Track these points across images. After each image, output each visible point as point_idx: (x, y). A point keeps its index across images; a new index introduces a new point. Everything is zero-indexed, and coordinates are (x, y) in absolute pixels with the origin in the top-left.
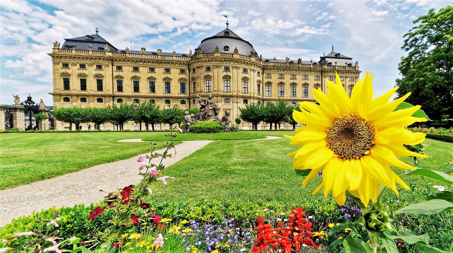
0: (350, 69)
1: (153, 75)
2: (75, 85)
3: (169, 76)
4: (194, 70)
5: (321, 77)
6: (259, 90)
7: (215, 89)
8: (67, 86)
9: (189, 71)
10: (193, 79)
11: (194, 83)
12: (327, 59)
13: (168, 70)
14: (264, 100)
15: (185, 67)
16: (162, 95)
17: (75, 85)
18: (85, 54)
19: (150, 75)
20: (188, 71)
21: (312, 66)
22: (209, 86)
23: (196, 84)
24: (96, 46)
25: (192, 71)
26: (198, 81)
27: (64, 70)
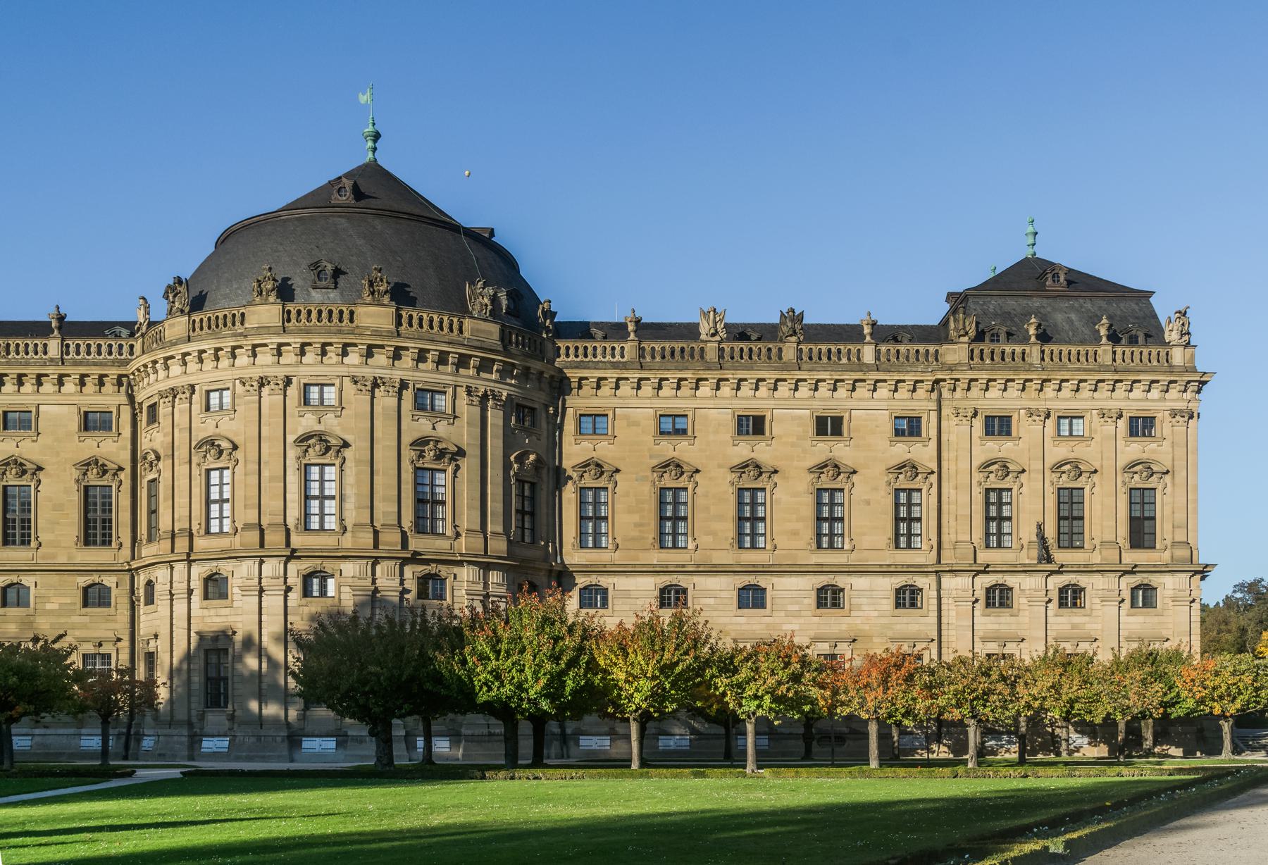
5: (934, 415)
7: (252, 517)
9: (134, 416)
15: (111, 399)
21: (868, 353)
22: (222, 501)
25: (144, 417)
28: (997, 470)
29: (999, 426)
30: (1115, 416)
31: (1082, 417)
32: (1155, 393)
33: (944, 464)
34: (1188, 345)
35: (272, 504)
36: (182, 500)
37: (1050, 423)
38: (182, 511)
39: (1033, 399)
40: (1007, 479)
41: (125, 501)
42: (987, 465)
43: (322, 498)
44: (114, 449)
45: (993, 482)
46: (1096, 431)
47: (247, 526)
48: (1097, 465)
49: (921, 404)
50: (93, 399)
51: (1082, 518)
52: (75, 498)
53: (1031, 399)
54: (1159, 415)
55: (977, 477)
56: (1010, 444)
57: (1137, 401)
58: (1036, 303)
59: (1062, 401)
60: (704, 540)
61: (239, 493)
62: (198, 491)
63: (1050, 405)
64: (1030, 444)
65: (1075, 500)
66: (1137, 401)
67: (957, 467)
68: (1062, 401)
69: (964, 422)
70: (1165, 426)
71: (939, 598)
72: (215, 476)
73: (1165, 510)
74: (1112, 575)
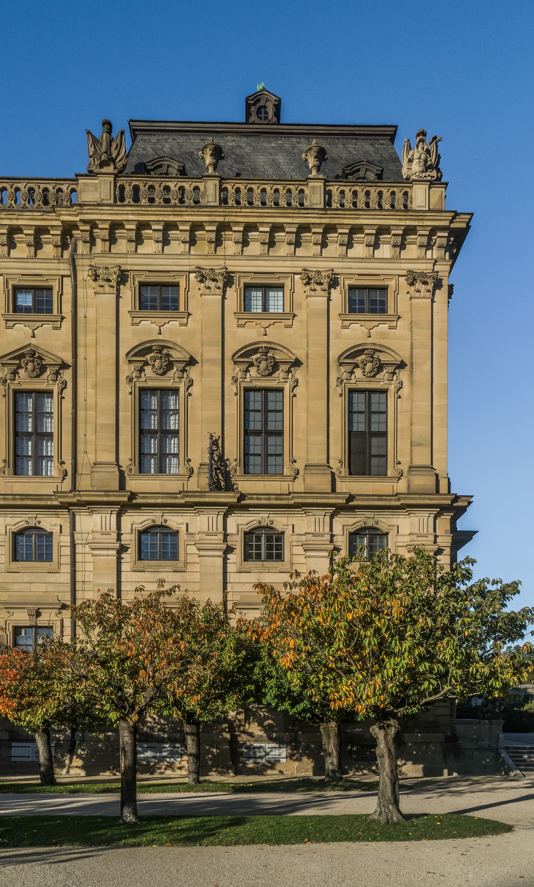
28: (154, 359)
29: (160, 296)
30: (326, 281)
31: (280, 287)
32: (385, 251)
33: (81, 351)
37: (233, 294)
39: (206, 257)
40: (170, 374)
42: (142, 351)
45: (150, 378)
46: (300, 306)
48: (301, 354)
49: (48, 264)
51: (280, 433)
53: (202, 256)
54: (392, 283)
55: (126, 370)
56: (174, 324)
57: (358, 262)
59: (251, 261)
63: (233, 266)
64: (202, 324)
65: (271, 406)
66: (358, 262)
67: (97, 355)
68: (251, 261)
69: (107, 289)
70: (404, 300)
71: (73, 546)
73: (405, 417)
74: (319, 513)
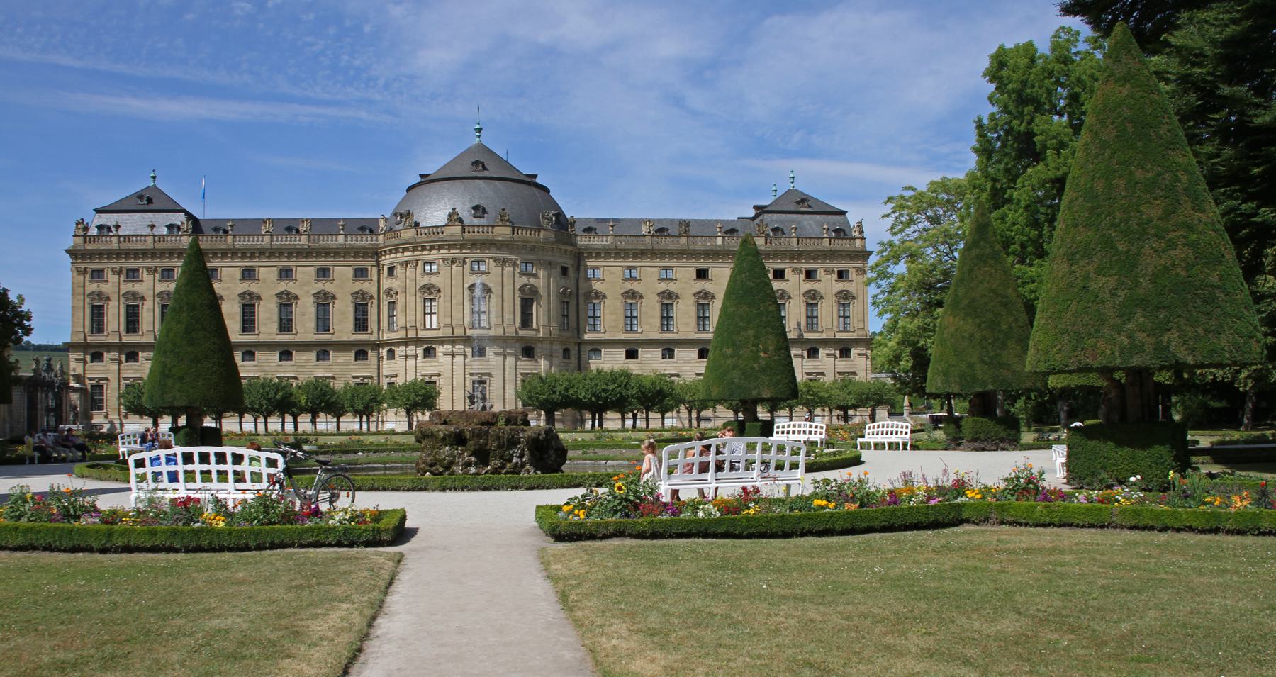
0: (841, 245)
1: (290, 287)
2: (114, 318)
3: (329, 287)
4: (391, 270)
6: (565, 316)
8: (98, 321)
10: (389, 293)
11: (392, 305)
12: (767, 217)
13: (323, 273)
14: (579, 344)
15: (368, 263)
16: (312, 337)
17: (114, 318)
18: (139, 246)
19: (283, 286)
20: (375, 270)
21: (720, 241)
23: (399, 306)
24: (162, 221)
26: (400, 300)
27: (92, 287)
34: (863, 238)
35: (457, 315)
36: (411, 313)
38: (411, 317)
41: (375, 310)
43: (479, 313)
44: (369, 287)
47: (446, 325)
50: (361, 263)
52: (351, 309)
58: (794, 216)
60: (646, 327)
61: (441, 310)
62: (420, 309)
72: (428, 304)
